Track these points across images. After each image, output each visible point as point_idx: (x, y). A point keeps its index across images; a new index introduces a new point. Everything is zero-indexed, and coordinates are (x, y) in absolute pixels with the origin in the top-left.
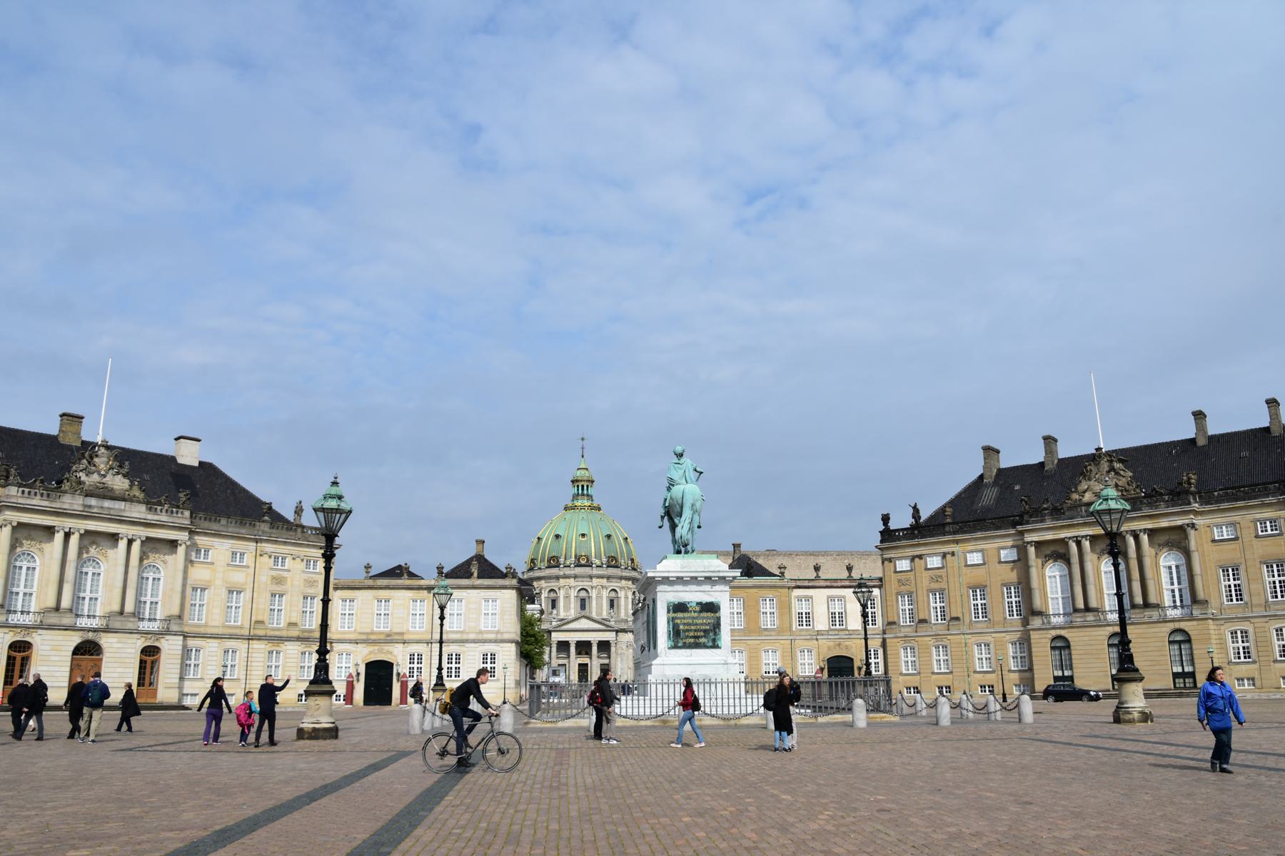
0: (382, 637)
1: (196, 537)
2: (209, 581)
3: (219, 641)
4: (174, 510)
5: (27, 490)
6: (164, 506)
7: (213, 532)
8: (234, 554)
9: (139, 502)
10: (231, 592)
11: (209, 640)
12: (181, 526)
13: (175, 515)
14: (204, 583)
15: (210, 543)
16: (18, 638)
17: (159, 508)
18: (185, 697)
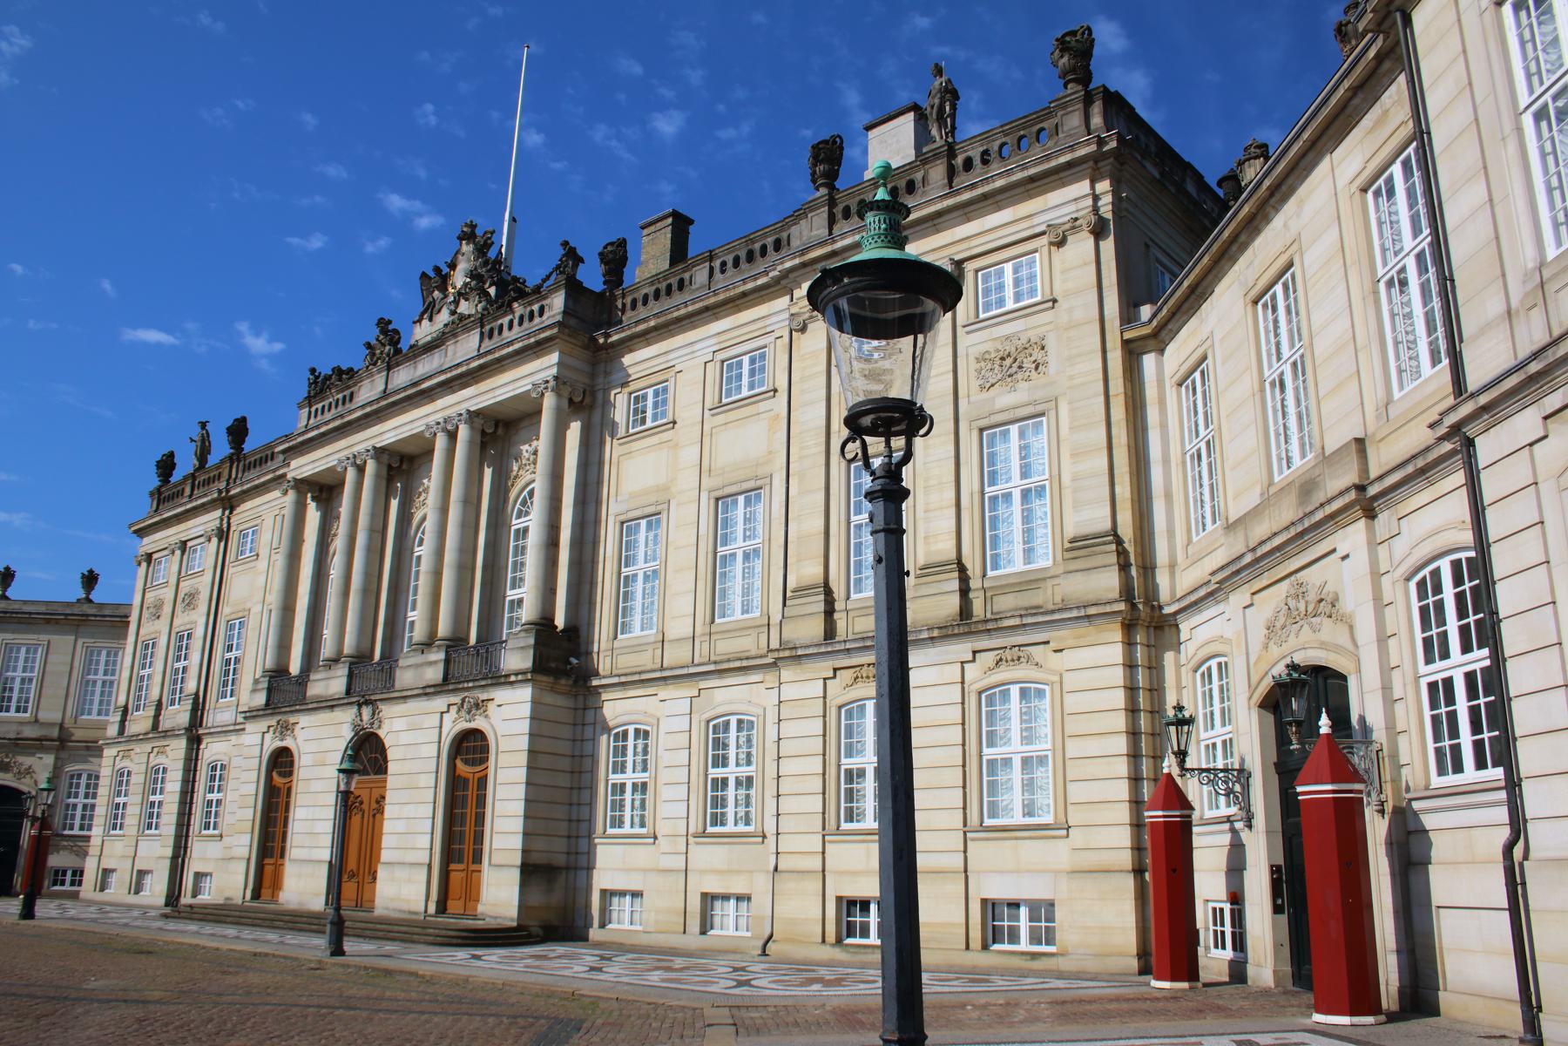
0: (1286, 512)
1: (627, 360)
2: (666, 488)
3: (685, 691)
4: (536, 307)
5: (320, 406)
6: (513, 312)
7: (652, 323)
8: (730, 368)
9: (467, 330)
10: (722, 501)
11: (665, 692)
12: (526, 342)
13: (537, 320)
14: (653, 499)
15: (658, 364)
16: (280, 744)
17: (505, 321)
18: (615, 900)
